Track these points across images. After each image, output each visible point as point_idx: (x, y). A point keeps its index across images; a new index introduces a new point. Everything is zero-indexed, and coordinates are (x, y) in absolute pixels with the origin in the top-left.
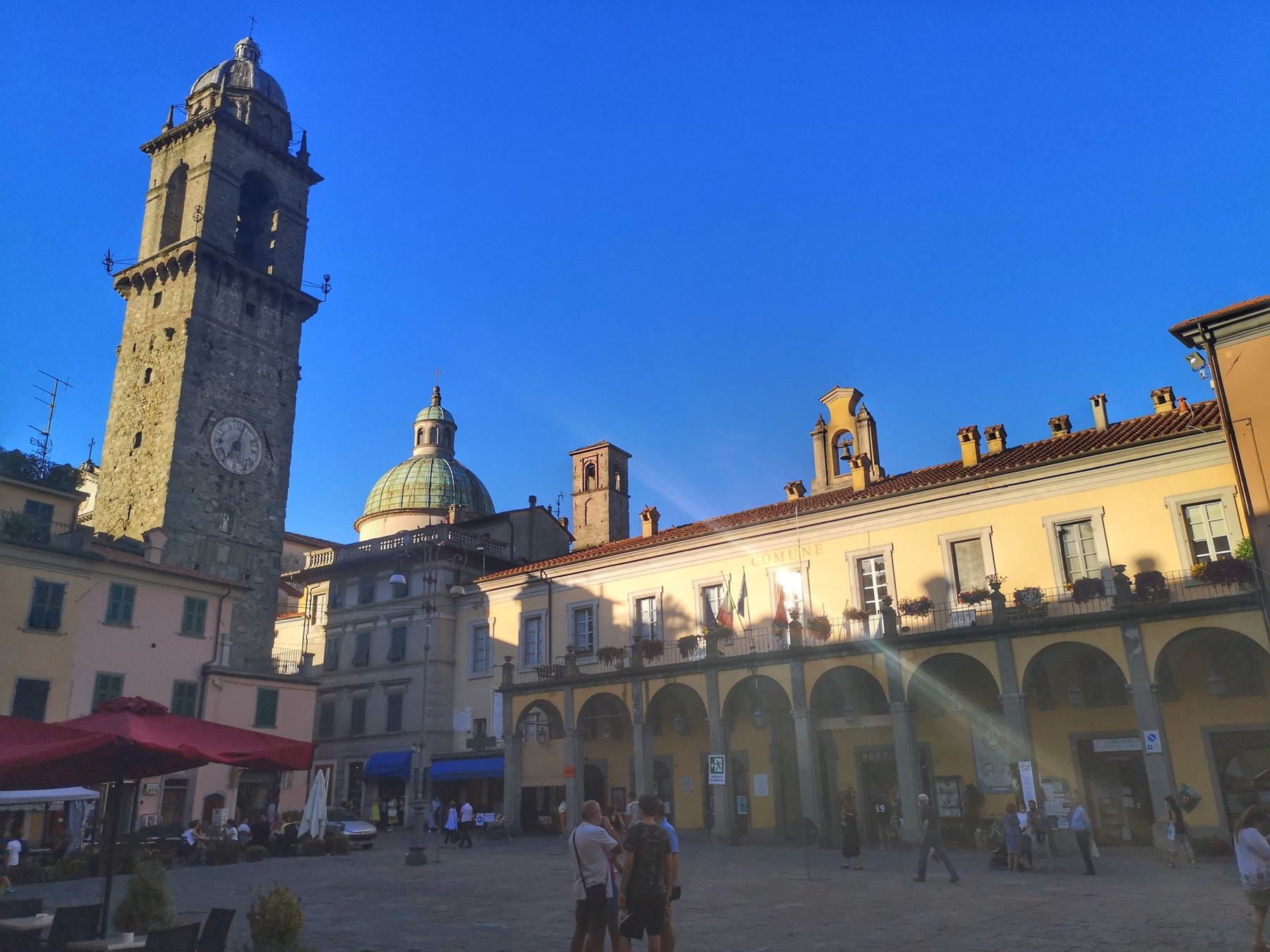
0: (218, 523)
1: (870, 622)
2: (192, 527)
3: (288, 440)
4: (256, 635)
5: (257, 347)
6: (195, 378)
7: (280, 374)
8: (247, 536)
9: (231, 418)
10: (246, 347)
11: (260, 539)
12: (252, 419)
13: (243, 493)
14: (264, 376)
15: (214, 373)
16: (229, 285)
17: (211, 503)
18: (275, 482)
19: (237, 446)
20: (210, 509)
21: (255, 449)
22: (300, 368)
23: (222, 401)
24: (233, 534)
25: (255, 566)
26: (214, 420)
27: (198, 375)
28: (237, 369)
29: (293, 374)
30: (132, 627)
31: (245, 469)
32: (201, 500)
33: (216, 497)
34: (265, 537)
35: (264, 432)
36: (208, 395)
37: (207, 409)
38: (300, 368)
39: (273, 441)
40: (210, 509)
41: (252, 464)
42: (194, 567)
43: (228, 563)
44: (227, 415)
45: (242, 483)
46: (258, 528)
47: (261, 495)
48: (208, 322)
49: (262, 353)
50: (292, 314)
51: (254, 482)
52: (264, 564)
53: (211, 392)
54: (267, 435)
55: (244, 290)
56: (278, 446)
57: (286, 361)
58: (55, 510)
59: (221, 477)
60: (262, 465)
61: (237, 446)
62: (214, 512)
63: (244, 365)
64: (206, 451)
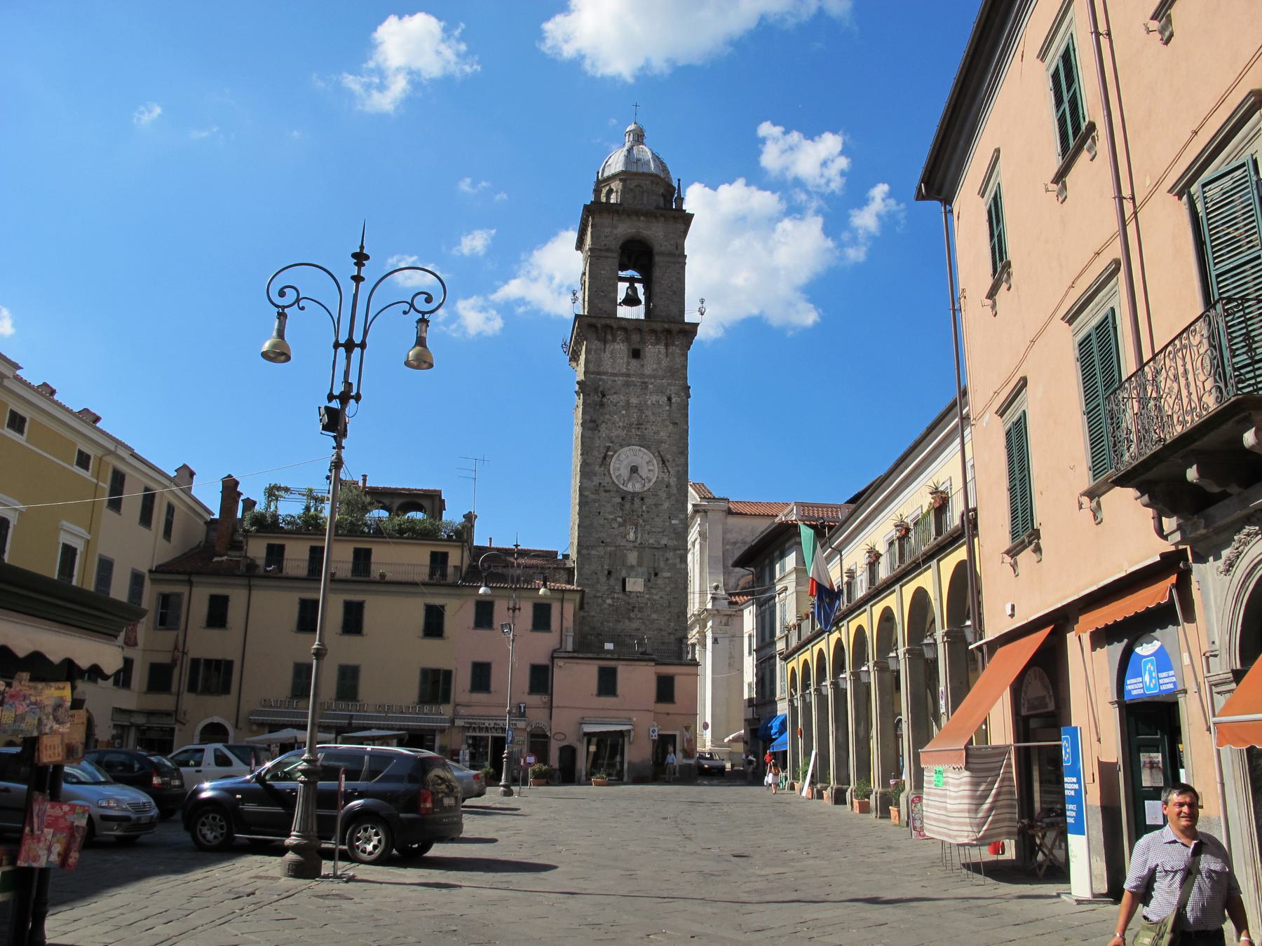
0: (624, 536)
1: (71, 700)
2: (602, 542)
3: (683, 452)
4: (669, 620)
5: (645, 383)
6: (591, 425)
7: (669, 399)
8: (651, 541)
9: (627, 448)
10: (636, 385)
11: (664, 541)
12: (644, 443)
13: (644, 507)
14: (653, 404)
15: (607, 416)
16: (614, 341)
17: (616, 520)
18: (674, 491)
19: (634, 470)
20: (615, 525)
21: (651, 468)
22: (689, 387)
23: (618, 436)
24: (639, 541)
25: (662, 564)
26: (612, 453)
27: (594, 421)
28: (628, 405)
29: (683, 394)
30: (494, 629)
31: (644, 486)
32: (607, 519)
33: (620, 515)
34: (669, 539)
35: (659, 452)
36: (604, 436)
37: (605, 447)
38: (689, 387)
39: (668, 457)
40: (615, 525)
41: (650, 481)
42: (606, 573)
43: (638, 565)
44: (622, 446)
45: (642, 499)
46: (661, 532)
47: (662, 505)
48: (599, 377)
49: (650, 386)
50: (677, 343)
51: (653, 495)
52: (671, 561)
53: (607, 432)
54: (662, 453)
55: (627, 340)
56: (674, 460)
57: (675, 385)
58: (450, 555)
59: (623, 498)
60: (660, 479)
61: (634, 470)
62: (619, 527)
63: (634, 401)
64: (607, 479)
